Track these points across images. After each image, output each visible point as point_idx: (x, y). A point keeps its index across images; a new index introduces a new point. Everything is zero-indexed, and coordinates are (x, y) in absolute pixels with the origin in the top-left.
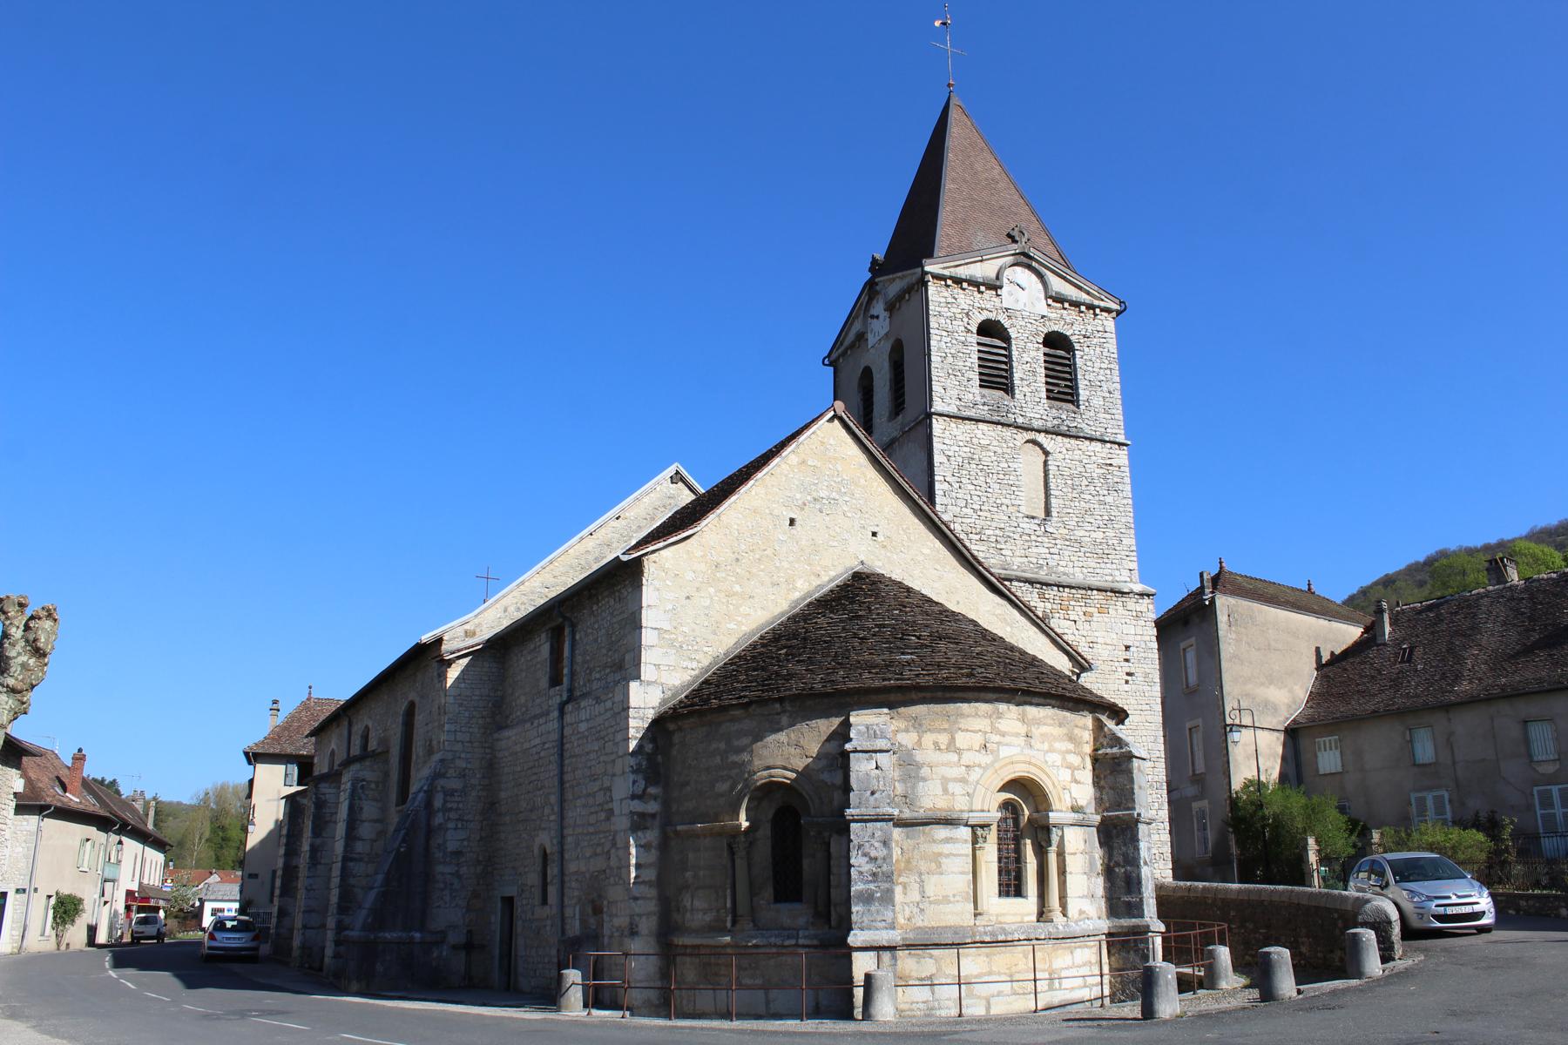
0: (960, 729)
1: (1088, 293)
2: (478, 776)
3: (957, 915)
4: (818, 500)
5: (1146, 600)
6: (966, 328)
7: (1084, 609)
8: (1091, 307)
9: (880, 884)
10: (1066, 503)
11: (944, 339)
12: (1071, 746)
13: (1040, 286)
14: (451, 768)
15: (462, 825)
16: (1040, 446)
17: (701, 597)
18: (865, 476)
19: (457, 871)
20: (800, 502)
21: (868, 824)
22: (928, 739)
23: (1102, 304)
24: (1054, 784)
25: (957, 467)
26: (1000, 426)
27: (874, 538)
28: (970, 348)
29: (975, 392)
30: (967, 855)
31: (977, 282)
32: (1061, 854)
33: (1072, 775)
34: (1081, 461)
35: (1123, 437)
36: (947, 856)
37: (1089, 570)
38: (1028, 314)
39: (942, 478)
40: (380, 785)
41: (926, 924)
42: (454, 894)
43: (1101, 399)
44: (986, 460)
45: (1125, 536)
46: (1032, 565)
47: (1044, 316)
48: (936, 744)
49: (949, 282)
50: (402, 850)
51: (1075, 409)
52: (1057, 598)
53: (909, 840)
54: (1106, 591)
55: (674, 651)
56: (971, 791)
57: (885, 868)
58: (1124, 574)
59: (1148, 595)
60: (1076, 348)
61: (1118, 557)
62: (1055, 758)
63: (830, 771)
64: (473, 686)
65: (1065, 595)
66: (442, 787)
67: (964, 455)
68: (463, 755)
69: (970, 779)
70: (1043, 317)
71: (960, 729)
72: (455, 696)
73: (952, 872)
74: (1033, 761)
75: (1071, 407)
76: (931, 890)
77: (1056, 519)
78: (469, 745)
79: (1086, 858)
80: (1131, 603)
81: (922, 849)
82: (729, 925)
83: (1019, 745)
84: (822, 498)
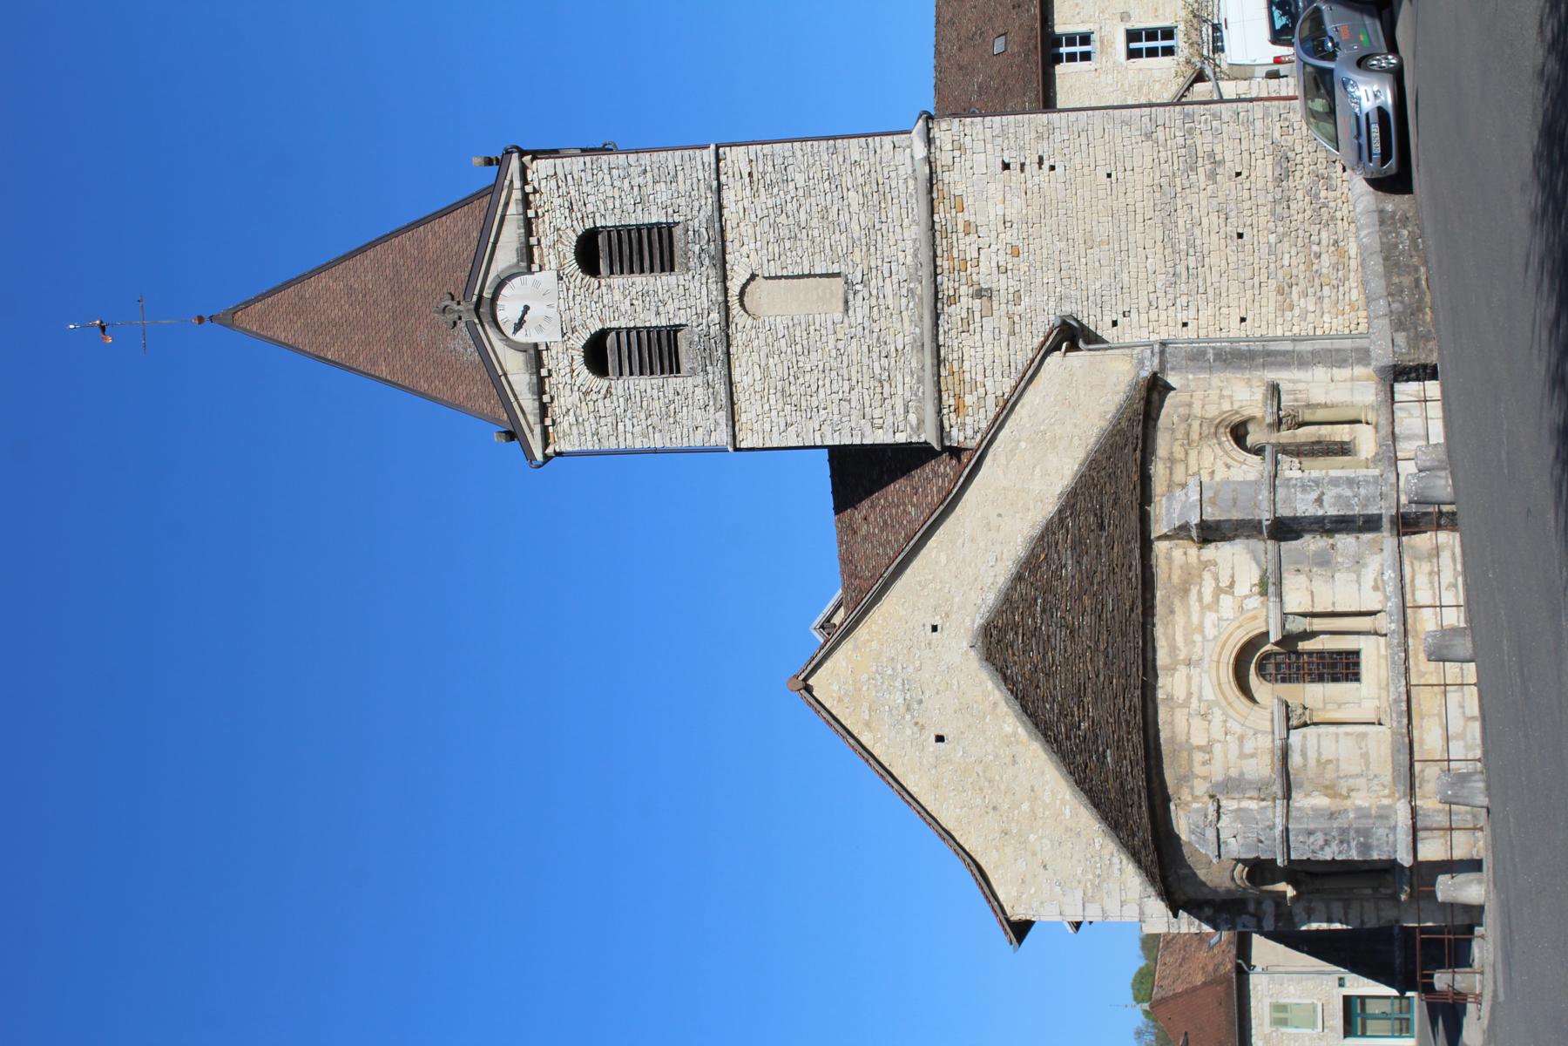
0: (1187, 741)
1: (507, 204)
3: (1380, 742)
4: (908, 705)
5: (935, 133)
6: (605, 398)
8: (526, 202)
10: (817, 250)
12: (1194, 591)
13: (516, 281)
17: (1041, 850)
18: (868, 641)
20: (915, 729)
22: (1199, 769)
23: (517, 184)
25: (799, 413)
26: (732, 350)
27: (939, 628)
31: (538, 383)
34: (755, 225)
35: (705, 152)
36: (1320, 754)
37: (904, 216)
38: (561, 301)
39: (818, 434)
43: (657, 187)
44: (781, 371)
45: (847, 156)
46: (911, 305)
47: (558, 275)
48: (1204, 763)
49: (548, 422)
51: (681, 226)
52: (952, 276)
53: (1305, 786)
54: (932, 200)
55: (1105, 885)
56: (1252, 732)
57: (1334, 833)
58: (901, 158)
59: (929, 130)
60: (592, 226)
61: (879, 169)
62: (1210, 617)
65: (946, 265)
67: (780, 401)
71: (1187, 741)
74: (1215, 657)
75: (677, 232)
76: (1356, 770)
77: (843, 266)
80: (943, 158)
83: (1200, 675)
84: (905, 699)
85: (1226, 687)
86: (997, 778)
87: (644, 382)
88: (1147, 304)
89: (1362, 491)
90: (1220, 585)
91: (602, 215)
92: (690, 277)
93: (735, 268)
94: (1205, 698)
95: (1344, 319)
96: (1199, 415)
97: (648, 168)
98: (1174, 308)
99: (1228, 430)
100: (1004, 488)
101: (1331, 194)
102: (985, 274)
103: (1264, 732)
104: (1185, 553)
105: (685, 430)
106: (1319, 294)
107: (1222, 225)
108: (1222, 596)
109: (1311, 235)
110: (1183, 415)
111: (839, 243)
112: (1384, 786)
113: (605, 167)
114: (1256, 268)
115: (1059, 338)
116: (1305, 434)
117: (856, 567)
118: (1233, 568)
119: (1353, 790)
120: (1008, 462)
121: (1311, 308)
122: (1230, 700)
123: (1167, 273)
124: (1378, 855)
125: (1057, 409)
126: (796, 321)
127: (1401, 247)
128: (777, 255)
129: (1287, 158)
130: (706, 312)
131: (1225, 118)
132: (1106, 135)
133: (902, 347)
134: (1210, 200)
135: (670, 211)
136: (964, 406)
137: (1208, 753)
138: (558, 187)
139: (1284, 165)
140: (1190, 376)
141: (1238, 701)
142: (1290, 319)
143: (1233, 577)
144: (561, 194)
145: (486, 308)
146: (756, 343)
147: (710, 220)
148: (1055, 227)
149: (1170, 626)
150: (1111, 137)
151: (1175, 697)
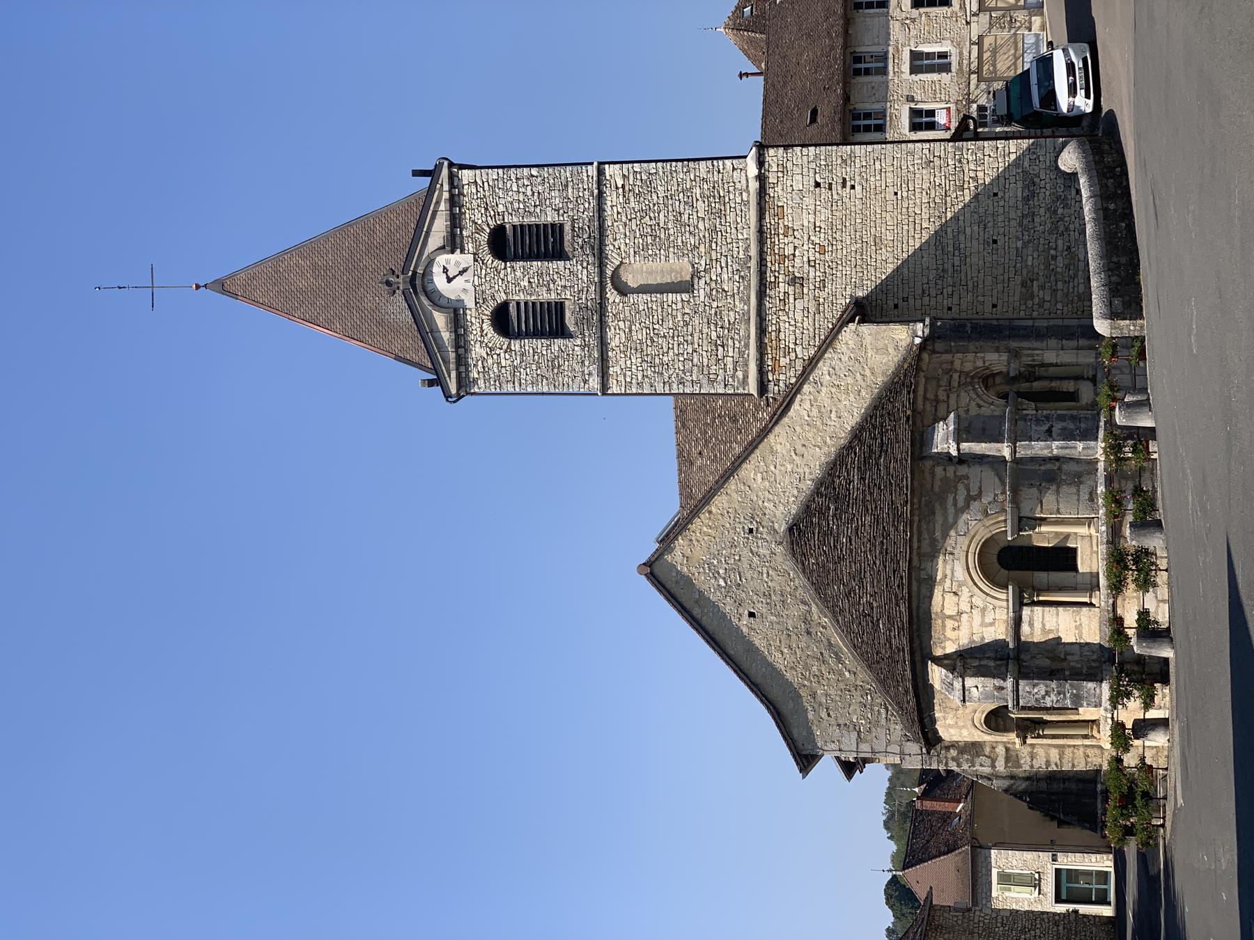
1: (438, 203)
9: (1066, 690)
21: (1020, 694)
22: (949, 633)
23: (446, 187)
28: (527, 348)
30: (1043, 611)
31: (455, 339)
34: (625, 224)
35: (589, 167)
36: (1043, 625)
37: (739, 220)
38: (476, 277)
50: (1028, 799)
56: (991, 607)
69: (982, 606)
74: (965, 548)
88: (920, 291)
89: (1083, 425)
90: (971, 494)
92: (575, 262)
95: (1073, 307)
96: (958, 369)
98: (942, 295)
99: (981, 380)
102: (799, 266)
104: (945, 470)
106: (1054, 287)
107: (981, 233)
109: (1049, 242)
110: (946, 369)
111: (688, 240)
113: (513, 177)
114: (1007, 266)
115: (853, 312)
116: (1038, 385)
117: (692, 491)
118: (981, 482)
119: (1069, 654)
121: (1047, 298)
123: (937, 269)
127: (1119, 235)
129: (1033, 183)
134: (973, 214)
136: (779, 366)
139: (1031, 189)
140: (953, 344)
142: (1030, 306)
143: (980, 488)
144: (479, 196)
148: (852, 233)
149: (931, 524)
150: (899, 164)
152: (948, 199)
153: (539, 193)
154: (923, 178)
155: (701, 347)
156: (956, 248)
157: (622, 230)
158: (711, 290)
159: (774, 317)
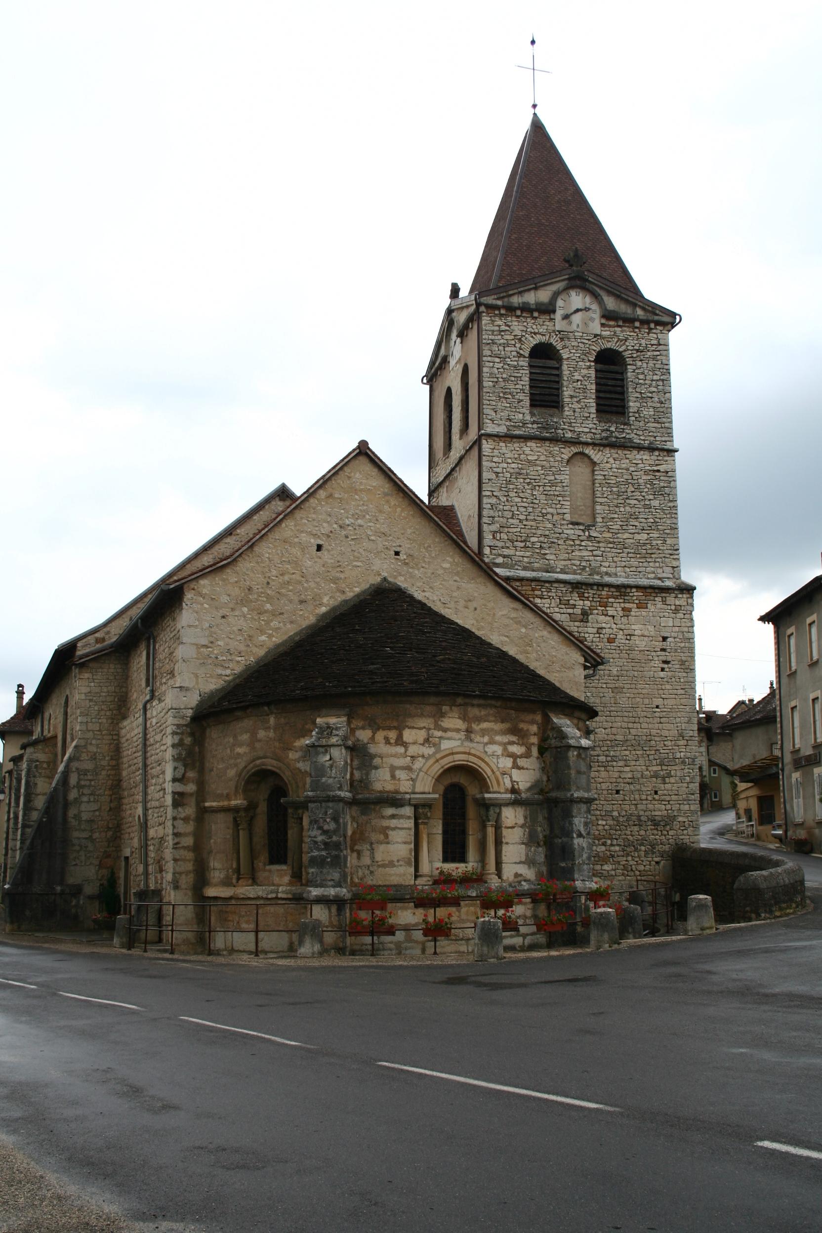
2: (107, 758)
6: (518, 353)
7: (622, 605)
10: (611, 509)
11: (497, 365)
12: (514, 738)
14: (82, 752)
15: (95, 799)
16: (589, 457)
19: (91, 836)
22: (380, 735)
23: (656, 318)
24: (492, 771)
29: (524, 413)
30: (409, 829)
32: (498, 828)
33: (515, 762)
34: (628, 469)
37: (632, 569)
38: (581, 334)
40: (52, 764)
41: (374, 883)
42: (88, 855)
45: (669, 536)
46: (575, 567)
47: (598, 335)
49: (503, 311)
50: (44, 820)
52: (596, 596)
56: (414, 777)
62: (498, 750)
63: (304, 761)
64: (101, 684)
65: (604, 593)
66: (77, 769)
67: (512, 471)
68: (94, 742)
70: (596, 336)
72: (85, 694)
73: (397, 842)
74: (473, 751)
76: (379, 857)
77: (600, 524)
78: (98, 733)
79: (525, 831)
80: (671, 599)
81: (373, 824)
82: (234, 881)
83: (460, 739)
84: (348, 525)
85: (450, 758)
86: (291, 588)
87: (526, 379)
91: (634, 370)
93: (600, 453)
94: (442, 741)
97: (663, 405)
100: (494, 614)
101: (642, 854)
103: (414, 786)
105: (494, 403)
107: (625, 781)
108: (512, 760)
112: (361, 879)
118: (527, 769)
120: (512, 619)
122: (441, 761)
124: (313, 873)
125: (547, 656)
126: (566, 488)
128: (608, 481)
130: (572, 429)
131: (691, 785)
132: (683, 707)
133: (548, 558)
135: (637, 415)
137: (396, 742)
138: (652, 345)
139: (662, 823)
141: (440, 767)
143: (523, 768)
145: (578, 282)
146: (552, 459)
147: (630, 440)
148: (626, 668)
149: (493, 719)
151: (443, 719)
152: (653, 752)
153: (652, 398)
154: (670, 730)
155: (523, 527)
156: (614, 759)
157: (624, 466)
158: (573, 540)
159: (554, 595)
